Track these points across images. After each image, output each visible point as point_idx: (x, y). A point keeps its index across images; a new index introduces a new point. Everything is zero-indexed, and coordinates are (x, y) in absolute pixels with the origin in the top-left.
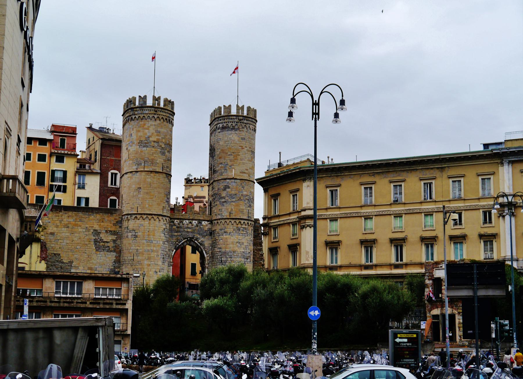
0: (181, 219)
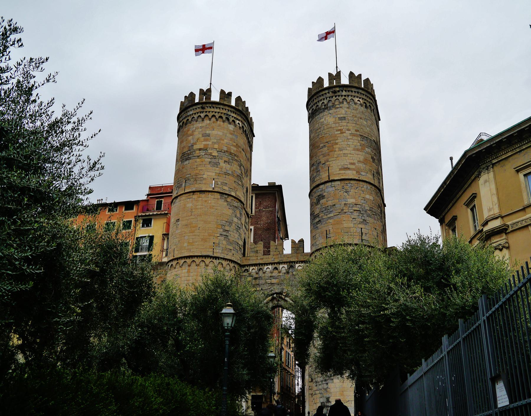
0: (259, 264)
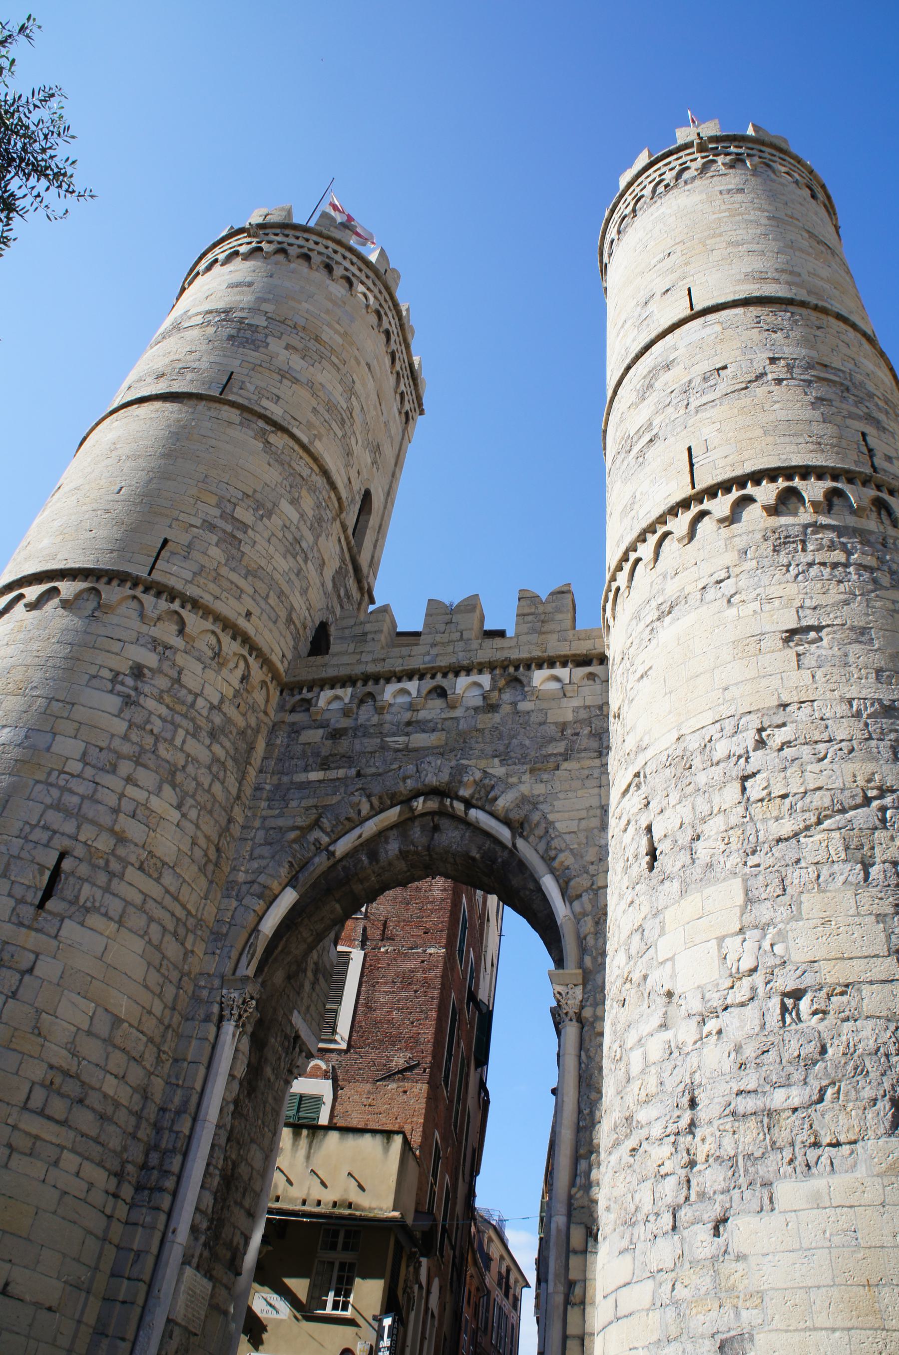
0: (366, 678)
